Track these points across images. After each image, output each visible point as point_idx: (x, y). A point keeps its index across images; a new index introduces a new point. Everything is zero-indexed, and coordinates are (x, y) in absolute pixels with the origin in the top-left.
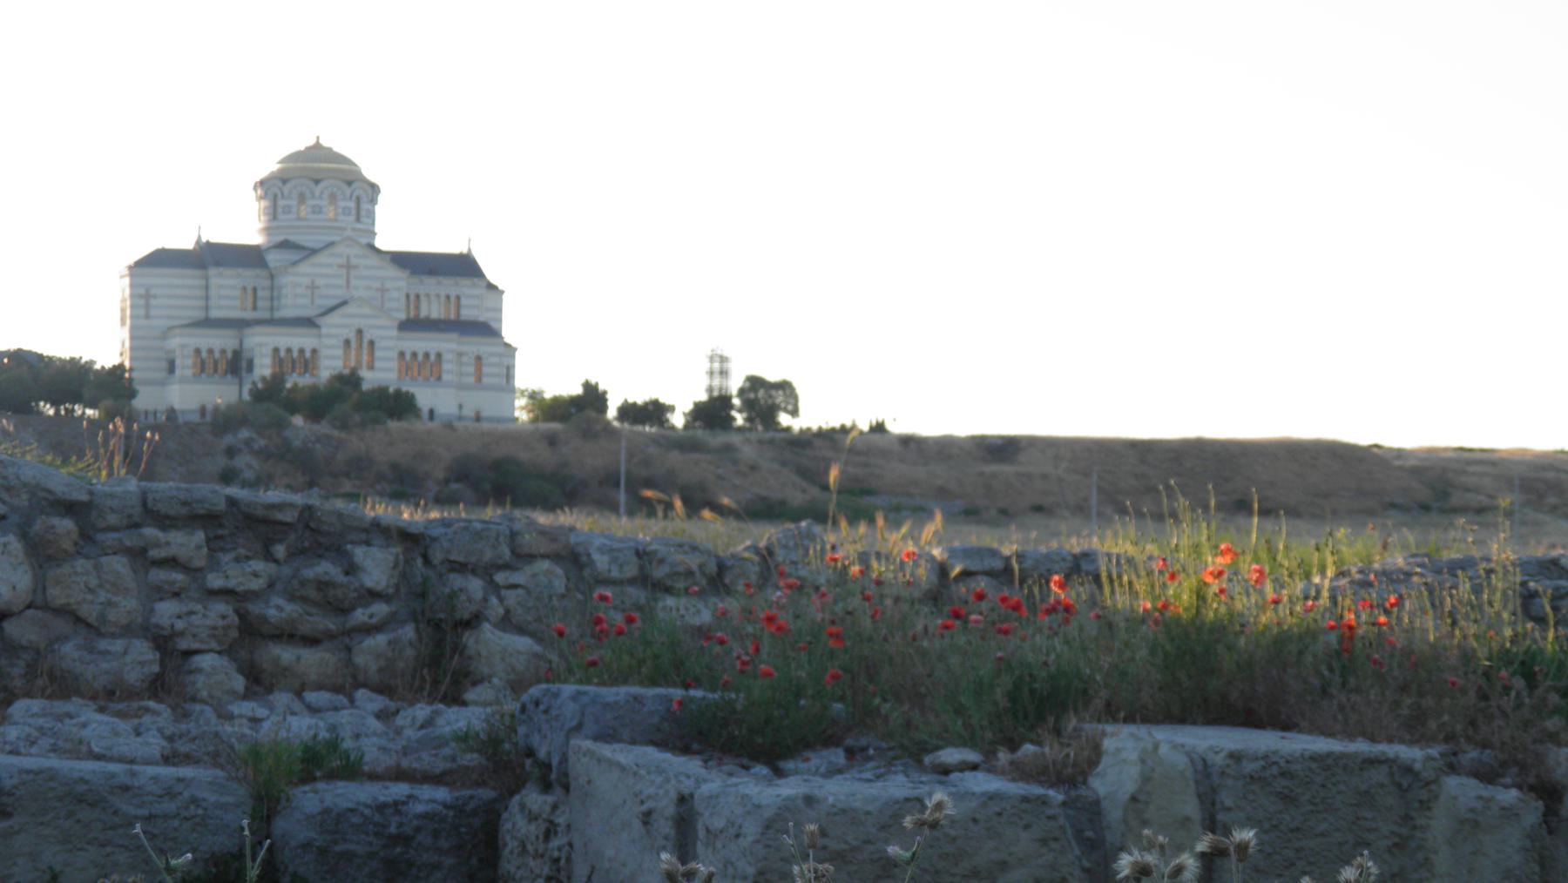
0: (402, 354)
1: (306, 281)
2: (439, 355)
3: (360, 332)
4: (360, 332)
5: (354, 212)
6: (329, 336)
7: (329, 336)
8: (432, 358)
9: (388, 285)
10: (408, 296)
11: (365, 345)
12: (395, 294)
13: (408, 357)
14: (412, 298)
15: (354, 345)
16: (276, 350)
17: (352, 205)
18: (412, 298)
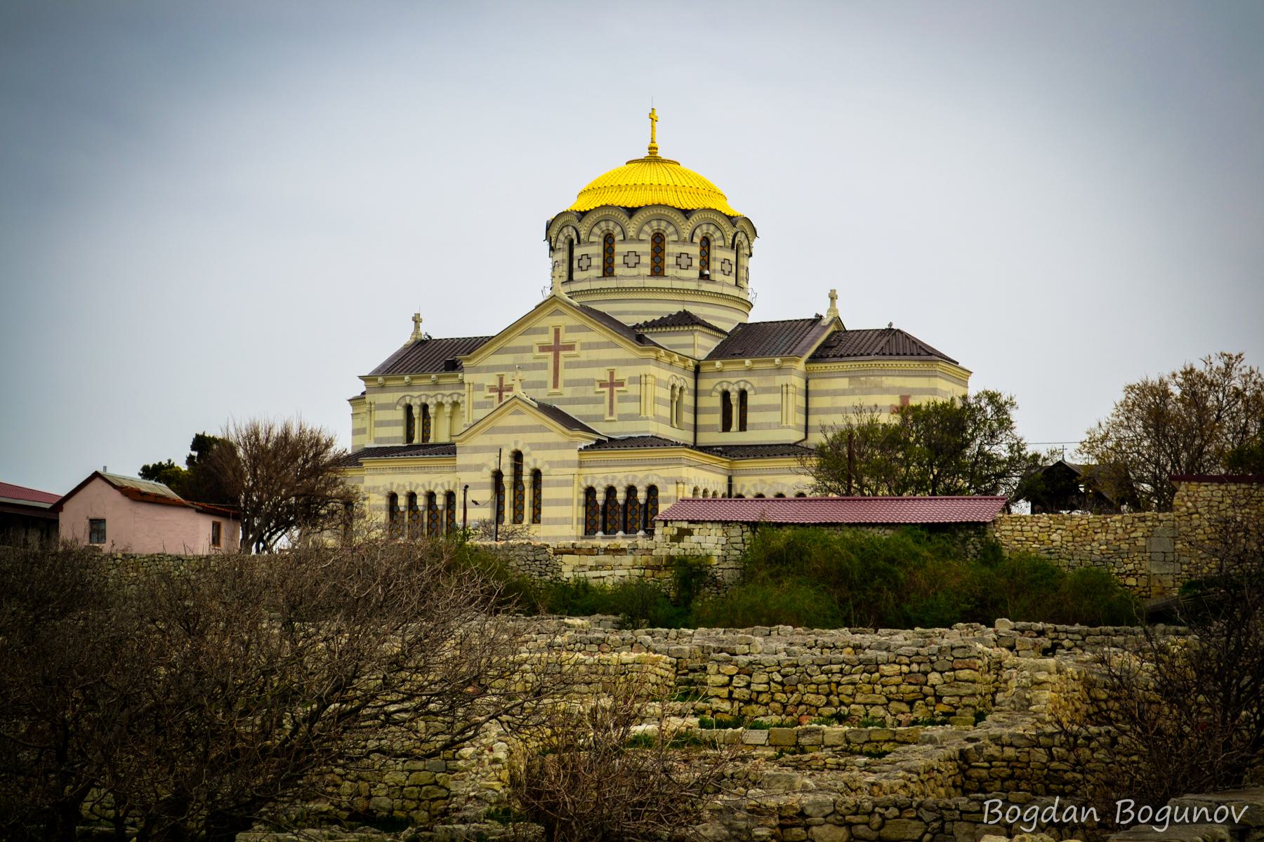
0: (590, 492)
1: (491, 380)
2: (652, 490)
3: (518, 456)
4: (518, 456)
5: (646, 260)
6: (467, 468)
7: (467, 468)
8: (642, 496)
9: (621, 374)
10: (726, 395)
11: (526, 478)
12: (633, 390)
13: (600, 497)
14: (734, 397)
15: (507, 480)
16: (393, 497)
17: (646, 248)
18: (734, 397)
